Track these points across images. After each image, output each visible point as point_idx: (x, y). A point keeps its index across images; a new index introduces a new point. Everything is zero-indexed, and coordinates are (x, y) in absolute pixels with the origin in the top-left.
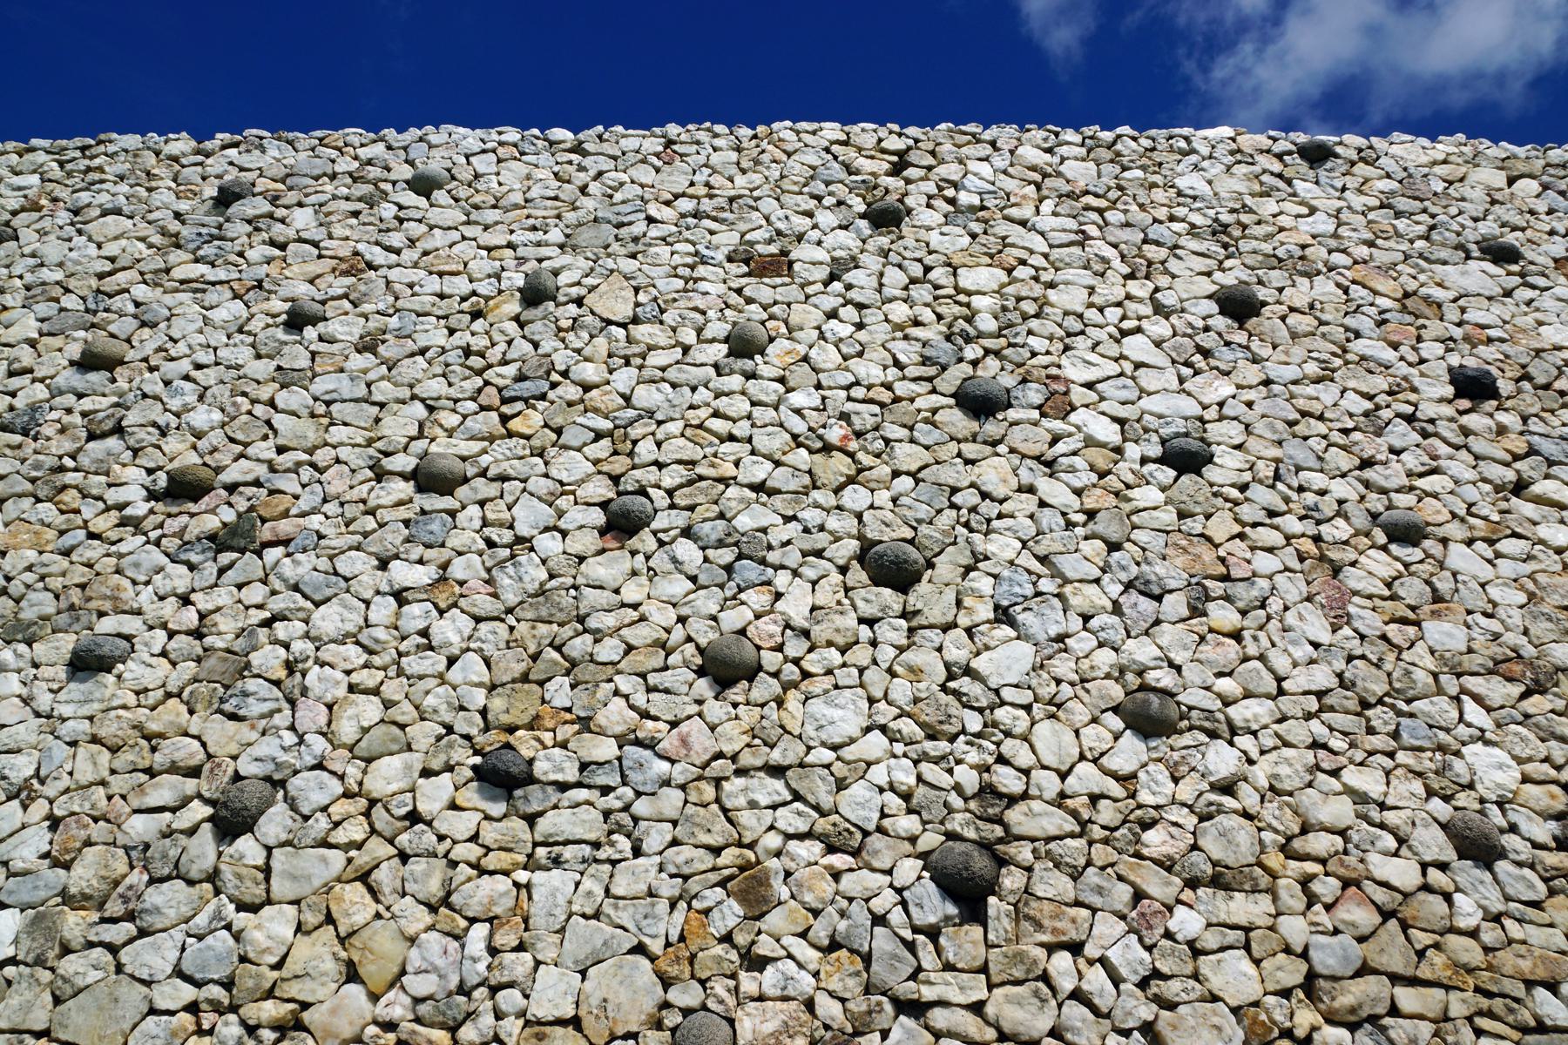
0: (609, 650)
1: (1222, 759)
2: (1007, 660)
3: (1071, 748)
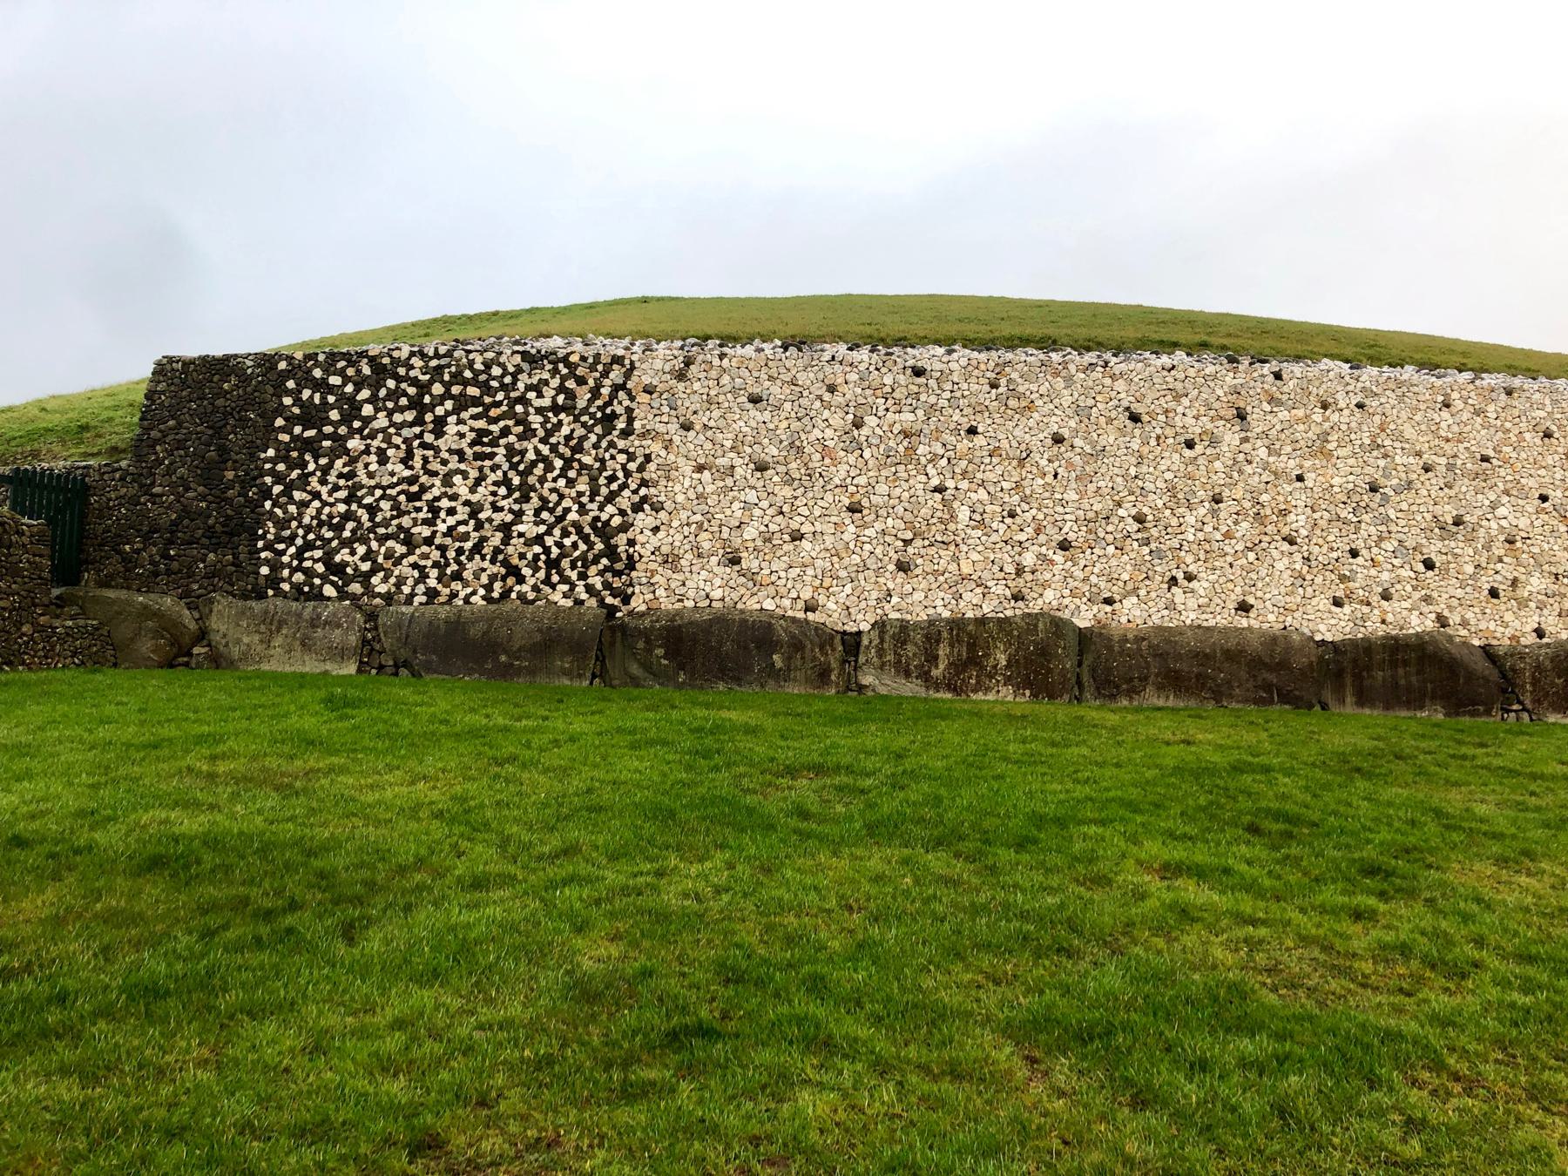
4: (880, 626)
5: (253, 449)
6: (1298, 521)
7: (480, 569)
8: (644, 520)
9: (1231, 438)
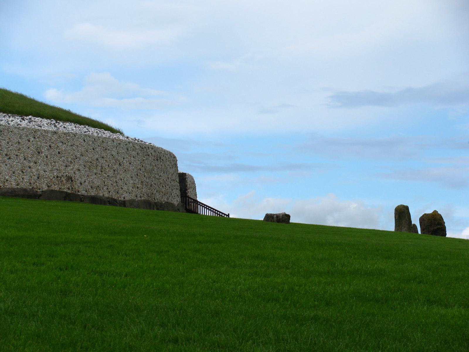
0: (25, 166)
1: (46, 173)
2: (40, 168)
3: (42, 172)
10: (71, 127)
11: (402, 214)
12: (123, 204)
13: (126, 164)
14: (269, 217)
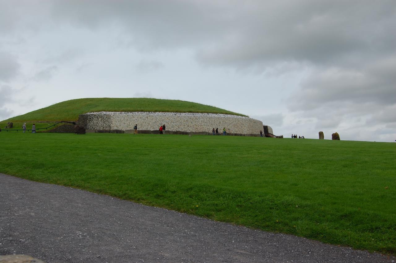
3: (221, 128)
4: (126, 130)
5: (87, 120)
6: (151, 124)
7: (102, 127)
8: (111, 124)
9: (147, 119)
10: (229, 116)
11: (321, 134)
12: (244, 135)
13: (245, 125)
14: (277, 137)
